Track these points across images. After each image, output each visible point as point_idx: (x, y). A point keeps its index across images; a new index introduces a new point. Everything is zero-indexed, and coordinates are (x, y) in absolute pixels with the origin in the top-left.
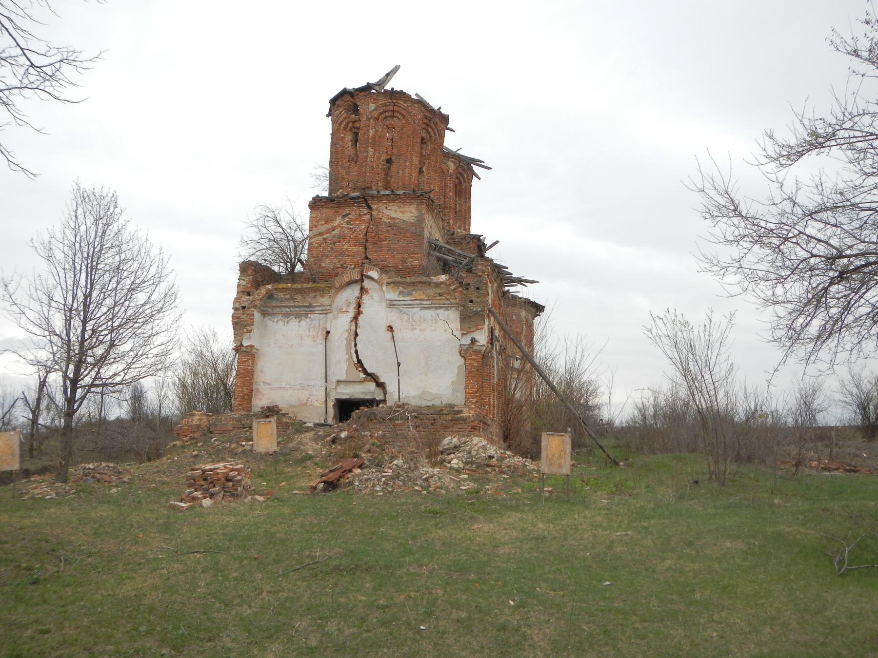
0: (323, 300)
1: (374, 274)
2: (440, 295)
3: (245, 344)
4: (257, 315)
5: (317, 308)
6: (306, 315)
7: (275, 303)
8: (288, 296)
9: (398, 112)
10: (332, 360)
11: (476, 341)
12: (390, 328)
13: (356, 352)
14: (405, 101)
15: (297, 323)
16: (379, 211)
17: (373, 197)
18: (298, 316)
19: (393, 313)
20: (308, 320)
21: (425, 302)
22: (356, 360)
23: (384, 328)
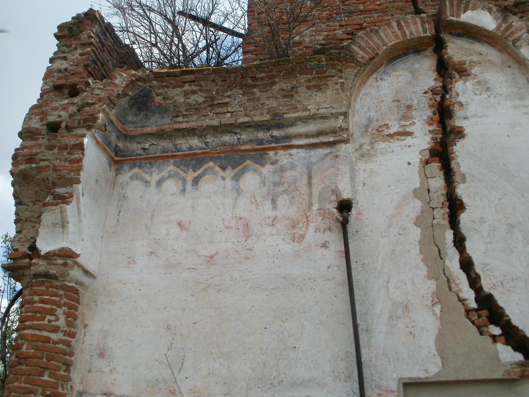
0: (319, 97)
3: (45, 246)
4: (93, 155)
5: (300, 129)
6: (260, 154)
7: (154, 123)
8: (199, 98)
10: (377, 305)
13: (467, 265)
15: (229, 183)
18: (233, 159)
20: (267, 170)
22: (469, 295)
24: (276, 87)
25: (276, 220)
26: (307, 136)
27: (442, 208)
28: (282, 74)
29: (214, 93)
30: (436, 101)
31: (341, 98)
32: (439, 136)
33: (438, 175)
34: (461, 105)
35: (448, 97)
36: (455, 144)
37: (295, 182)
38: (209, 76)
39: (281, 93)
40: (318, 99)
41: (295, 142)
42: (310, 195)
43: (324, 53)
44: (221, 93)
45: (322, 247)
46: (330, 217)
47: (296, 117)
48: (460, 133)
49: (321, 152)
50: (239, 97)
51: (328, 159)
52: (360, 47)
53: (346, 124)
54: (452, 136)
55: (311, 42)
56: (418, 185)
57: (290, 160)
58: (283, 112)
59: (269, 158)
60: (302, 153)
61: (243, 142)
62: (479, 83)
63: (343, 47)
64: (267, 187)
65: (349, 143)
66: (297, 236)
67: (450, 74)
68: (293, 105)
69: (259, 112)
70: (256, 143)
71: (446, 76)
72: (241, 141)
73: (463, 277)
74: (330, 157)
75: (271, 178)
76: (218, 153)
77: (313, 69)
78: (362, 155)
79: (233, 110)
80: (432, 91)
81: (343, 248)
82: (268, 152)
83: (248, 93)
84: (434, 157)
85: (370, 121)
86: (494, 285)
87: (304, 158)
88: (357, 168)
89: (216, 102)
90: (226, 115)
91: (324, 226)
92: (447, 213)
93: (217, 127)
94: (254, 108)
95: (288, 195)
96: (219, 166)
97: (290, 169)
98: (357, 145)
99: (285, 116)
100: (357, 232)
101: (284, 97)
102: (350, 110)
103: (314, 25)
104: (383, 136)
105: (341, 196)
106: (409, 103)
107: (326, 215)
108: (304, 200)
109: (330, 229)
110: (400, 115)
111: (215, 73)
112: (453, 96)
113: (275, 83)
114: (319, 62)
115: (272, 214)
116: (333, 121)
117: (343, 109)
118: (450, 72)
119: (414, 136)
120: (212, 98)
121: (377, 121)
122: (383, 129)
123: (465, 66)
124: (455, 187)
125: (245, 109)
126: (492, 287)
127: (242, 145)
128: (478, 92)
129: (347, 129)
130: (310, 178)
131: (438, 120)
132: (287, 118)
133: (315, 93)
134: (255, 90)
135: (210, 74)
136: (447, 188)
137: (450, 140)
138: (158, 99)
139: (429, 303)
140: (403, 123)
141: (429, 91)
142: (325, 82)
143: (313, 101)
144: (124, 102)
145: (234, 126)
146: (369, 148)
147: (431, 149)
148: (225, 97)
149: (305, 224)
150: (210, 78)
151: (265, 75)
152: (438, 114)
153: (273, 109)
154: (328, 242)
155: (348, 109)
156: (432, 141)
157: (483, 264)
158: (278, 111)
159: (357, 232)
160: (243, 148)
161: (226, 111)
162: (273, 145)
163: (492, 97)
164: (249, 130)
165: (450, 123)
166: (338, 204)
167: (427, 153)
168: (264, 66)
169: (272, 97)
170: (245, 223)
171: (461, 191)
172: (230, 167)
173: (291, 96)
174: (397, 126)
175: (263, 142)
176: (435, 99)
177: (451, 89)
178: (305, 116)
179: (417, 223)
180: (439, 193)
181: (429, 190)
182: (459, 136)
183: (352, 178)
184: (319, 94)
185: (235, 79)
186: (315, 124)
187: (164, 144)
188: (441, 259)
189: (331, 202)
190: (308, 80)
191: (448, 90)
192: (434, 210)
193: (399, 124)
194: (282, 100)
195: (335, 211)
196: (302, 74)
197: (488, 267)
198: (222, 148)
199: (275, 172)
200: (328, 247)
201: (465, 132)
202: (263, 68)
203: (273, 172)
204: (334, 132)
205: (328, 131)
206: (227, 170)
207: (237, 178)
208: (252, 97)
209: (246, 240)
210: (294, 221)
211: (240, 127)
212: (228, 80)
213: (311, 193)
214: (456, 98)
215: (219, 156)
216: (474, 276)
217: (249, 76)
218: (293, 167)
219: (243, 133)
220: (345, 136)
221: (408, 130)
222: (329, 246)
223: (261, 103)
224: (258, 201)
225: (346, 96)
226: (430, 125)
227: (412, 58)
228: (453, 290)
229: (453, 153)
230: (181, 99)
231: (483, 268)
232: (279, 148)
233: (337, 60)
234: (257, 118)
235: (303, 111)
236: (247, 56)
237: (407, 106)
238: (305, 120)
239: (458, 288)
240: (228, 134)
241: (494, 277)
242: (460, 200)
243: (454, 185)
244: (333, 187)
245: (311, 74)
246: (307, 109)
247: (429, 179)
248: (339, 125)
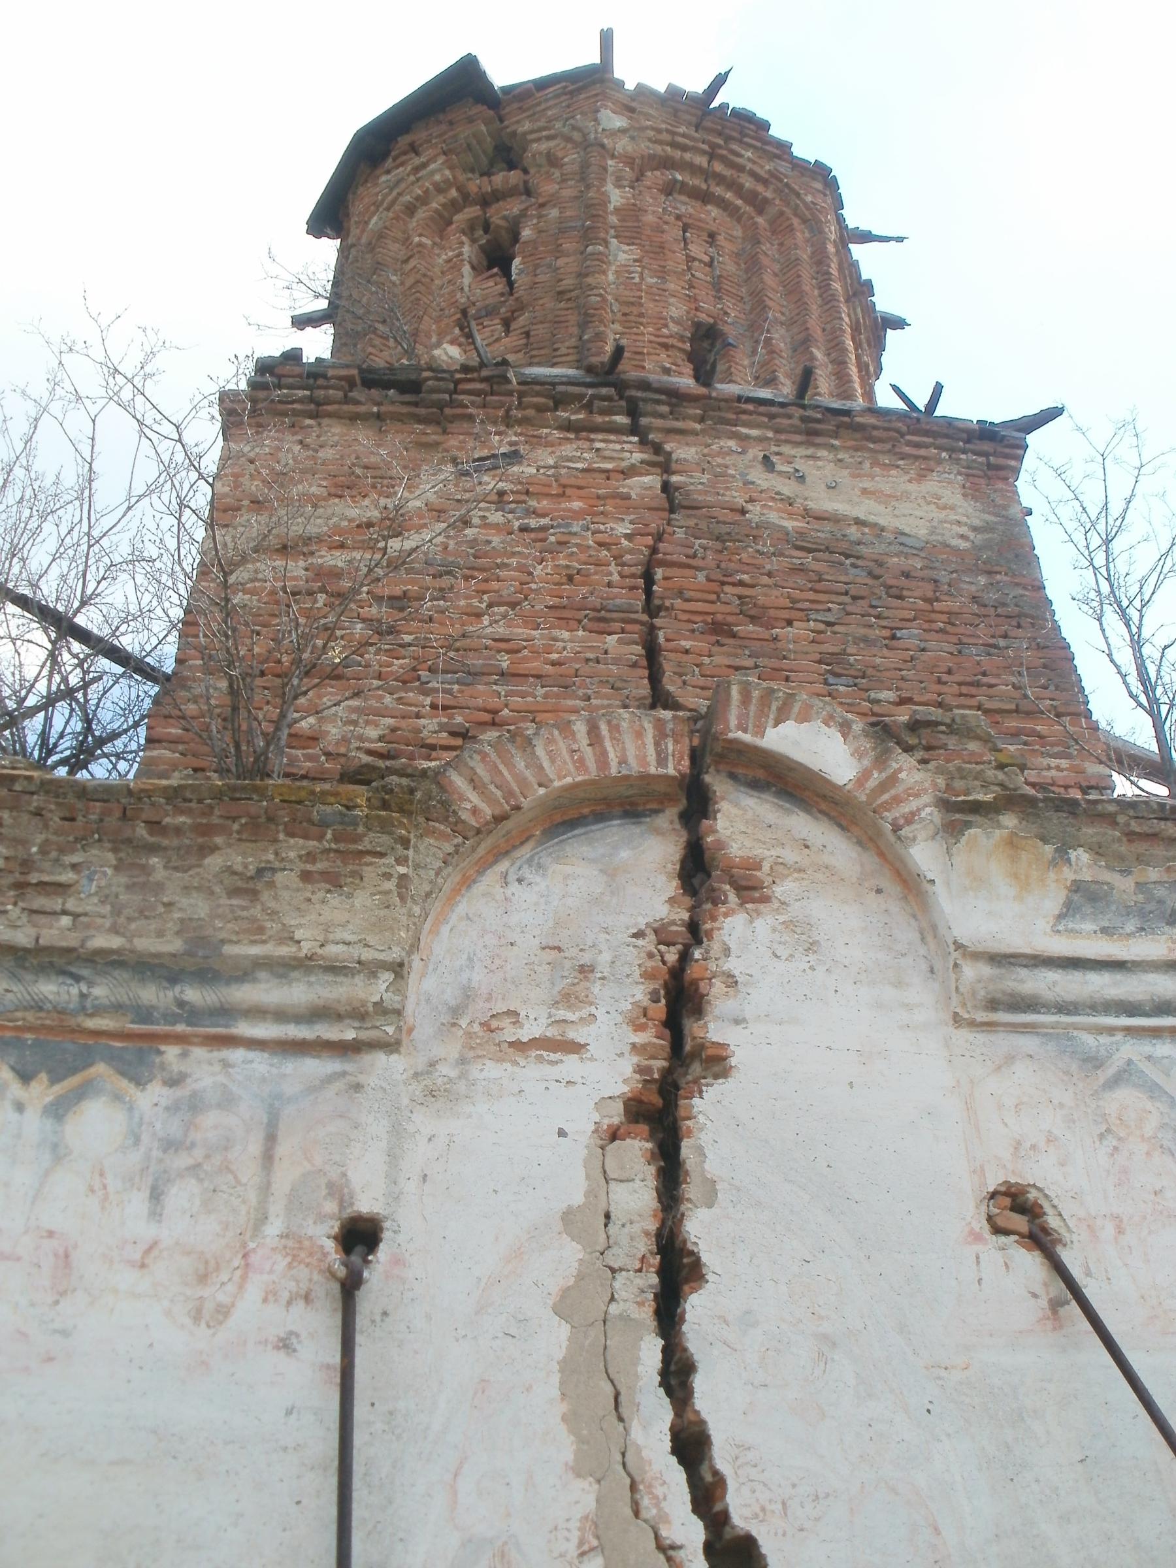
1: (823, 746)
6: (137, 1049)
12: (1021, 1215)
13: (690, 1445)
15: (33, 1123)
19: (1022, 1071)
20: (152, 1098)
23: (974, 1216)
24: (214, 862)
25: (155, 1253)
26: (281, 1015)
27: (640, 1270)
28: (236, 827)
29: (34, 849)
30: (664, 962)
31: (394, 919)
32: (659, 1064)
33: (640, 1176)
34: (731, 981)
35: (697, 954)
36: (701, 1092)
37: (227, 1145)
38: (27, 797)
39: (226, 882)
40: (327, 914)
42: (265, 1189)
43: (367, 783)
44: (54, 854)
45: (278, 1348)
46: (314, 1261)
47: (257, 957)
48: (717, 1063)
49: (314, 1067)
50: (105, 874)
51: (331, 1091)
52: (473, 781)
53: (397, 998)
54: (696, 1068)
55: (345, 740)
56: (578, 1199)
57: (221, 1079)
58: (223, 935)
59: (162, 1063)
60: (260, 1063)
61: (94, 1006)
62: (790, 925)
63: (424, 773)
64: (142, 1149)
65: (397, 1051)
66: (209, 1306)
67: (713, 890)
68: (253, 920)
69: (153, 927)
70: (130, 1017)
71: (703, 893)
72: (88, 1003)
73: (677, 1476)
74: (339, 1085)
75: (158, 1126)
76: (17, 1028)
77: (328, 827)
78: (432, 1093)
79: (80, 910)
80: (656, 931)
81: (337, 1359)
82: (163, 1048)
83: (133, 865)
84: (637, 1122)
85: (468, 994)
86: (763, 1509)
87: (264, 1080)
88: (411, 1128)
89: (34, 878)
90: (58, 920)
91: (292, 1285)
92: (651, 1286)
93: (26, 950)
94: (141, 912)
95: (200, 1180)
96: (13, 1068)
97: (219, 1106)
98: (421, 1063)
99: (228, 950)
100: (385, 1314)
101: (234, 892)
102: (415, 957)
103: (357, 694)
104: (499, 1045)
105: (352, 1204)
106: (586, 958)
107: (303, 1255)
108: (244, 1202)
109: (307, 1298)
110: (557, 989)
111: (47, 792)
112: (712, 954)
113: (214, 849)
114: (348, 808)
115: (145, 1231)
116: (361, 984)
117: (395, 954)
118: (716, 885)
119: (588, 1055)
120: (27, 865)
121: (489, 999)
122: (502, 1025)
123: (758, 874)
124: (683, 1215)
125: (117, 912)
126: (756, 1516)
127: (91, 1015)
128: (783, 952)
129: (399, 1013)
130: (271, 1139)
131: (663, 1016)
132: (230, 957)
133: (321, 894)
134: (154, 860)
135: (32, 793)
136: (660, 1215)
137: (690, 1078)
139: (572, 1549)
140: (562, 1014)
141: (648, 931)
142: (356, 868)
143: (313, 917)
145: (75, 955)
146: (453, 1074)
147: (630, 1099)
148: (63, 866)
149: (238, 1273)
150: (29, 803)
151: (189, 821)
152: (663, 1001)
153: (194, 924)
154: (297, 1336)
155: (410, 953)
156: (638, 1076)
157: (738, 1447)
158: (209, 932)
159: (385, 1314)
160: (91, 1024)
161: (58, 908)
162: (180, 1028)
163: (821, 969)
164: (116, 973)
165: (693, 1029)
166: (342, 1227)
167: (619, 1107)
168: (188, 795)
169: (198, 889)
170: (61, 1251)
171: (700, 1228)
172: (43, 1076)
173: (254, 894)
174: (543, 1021)
175: (151, 1014)
176: (662, 957)
177: (709, 934)
178: (283, 957)
179: (564, 1307)
180: (636, 1228)
181: (607, 1216)
182: (716, 1069)
183: (393, 1157)
184: (334, 900)
185: (101, 820)
186: (310, 984)
188: (621, 1419)
189: (321, 1218)
190: (308, 854)
191: (702, 934)
192: (616, 1275)
193: (550, 1016)
194: (224, 901)
195: (330, 1245)
196: (293, 835)
197: (751, 1456)
198: (30, 1016)
199: (173, 1108)
200: (295, 1350)
201: (733, 1061)
202: (185, 800)
203: (167, 1108)
204: (358, 1014)
205: (342, 1009)
206: (33, 1084)
207: (58, 1110)
208: (141, 879)
209: (57, 1302)
210: (207, 1262)
211: (93, 961)
212: (80, 818)
213: (269, 1184)
214: (720, 962)
215: (18, 1038)
216: (709, 1478)
217: (144, 816)
218: (227, 1101)
219: (98, 980)
220: (390, 1030)
221: (572, 1034)
222: (298, 1347)
223: (165, 900)
224: (110, 1189)
225: (410, 915)
226: (639, 1028)
227: (615, 831)
228: (644, 1514)
229: (689, 1118)
231: (737, 1458)
232: (196, 1040)
233: (401, 811)
234: (146, 944)
235: (281, 941)
236: (155, 753)
237: (582, 966)
239: (660, 1509)
240: (54, 978)
241: (765, 1485)
242: (692, 1253)
243: (683, 1208)
244: (334, 1174)
245: (320, 838)
246: (292, 938)
247: (613, 1185)
248: (376, 998)
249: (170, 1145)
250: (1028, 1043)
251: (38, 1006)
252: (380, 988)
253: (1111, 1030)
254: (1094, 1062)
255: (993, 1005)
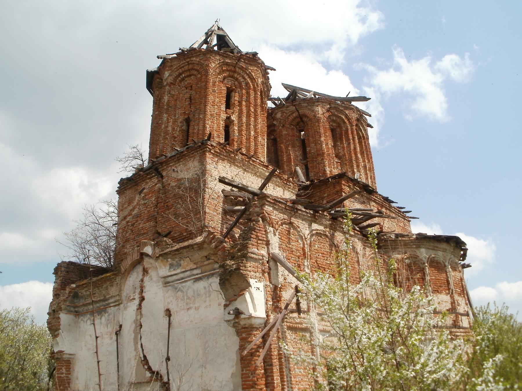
2: (207, 258)
7: (82, 302)
9: (192, 69)
11: (242, 313)
12: (168, 313)
14: (197, 56)
16: (168, 176)
17: (161, 163)
21: (195, 272)
22: (142, 356)
41: (112, 305)
49: (117, 307)
138: (80, 294)
144: (70, 298)
183: (122, 317)
187: (86, 308)
230: (85, 293)
238: (112, 297)
249: (108, 320)
250: (170, 288)
251: (97, 307)
252: (117, 298)
253: (178, 283)
254: (176, 288)
255: (166, 283)
